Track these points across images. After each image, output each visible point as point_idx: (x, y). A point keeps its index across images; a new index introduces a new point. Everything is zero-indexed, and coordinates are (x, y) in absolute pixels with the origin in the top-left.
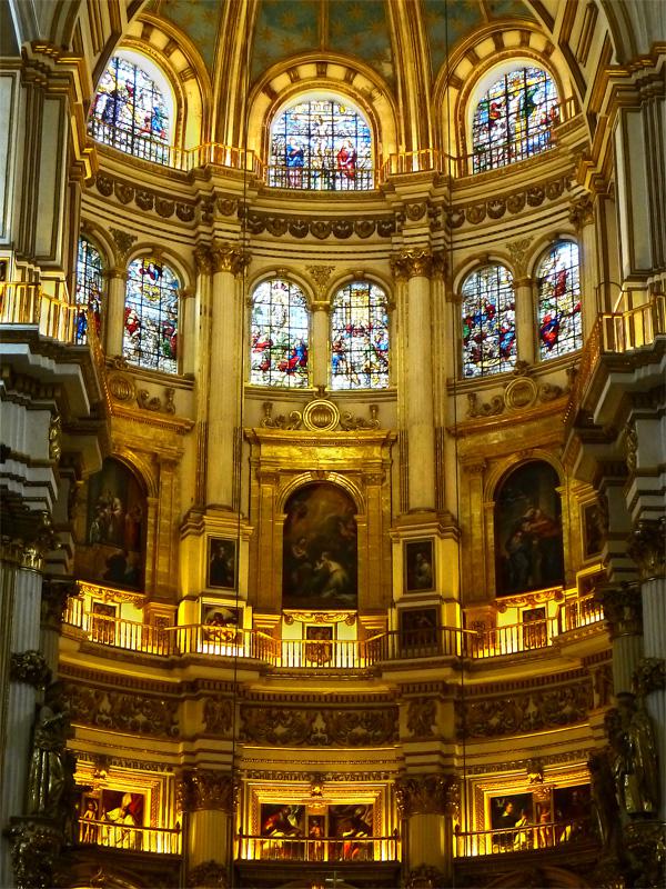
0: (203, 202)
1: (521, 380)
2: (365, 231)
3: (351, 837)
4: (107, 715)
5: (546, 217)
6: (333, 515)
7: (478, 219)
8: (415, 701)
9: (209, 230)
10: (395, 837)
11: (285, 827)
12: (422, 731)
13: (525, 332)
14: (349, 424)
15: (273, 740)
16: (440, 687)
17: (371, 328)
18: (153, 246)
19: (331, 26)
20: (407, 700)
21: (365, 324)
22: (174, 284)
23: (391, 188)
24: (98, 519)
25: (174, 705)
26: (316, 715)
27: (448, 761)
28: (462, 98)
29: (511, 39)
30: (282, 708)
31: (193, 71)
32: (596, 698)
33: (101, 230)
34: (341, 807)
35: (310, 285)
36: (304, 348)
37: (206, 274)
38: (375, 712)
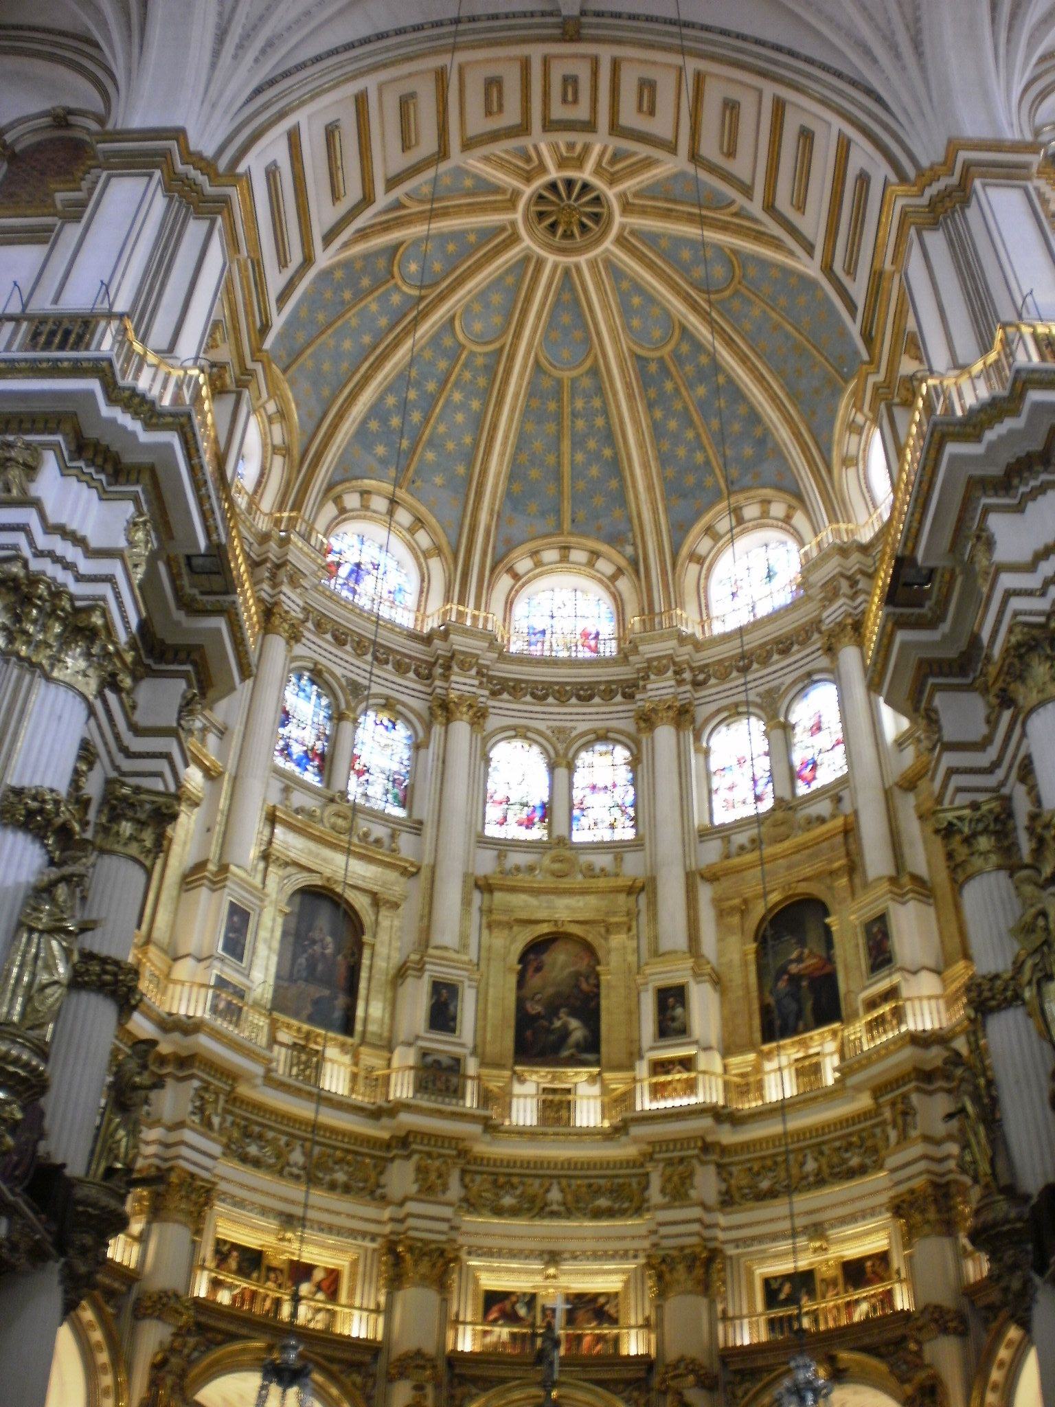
0: (441, 661)
1: (780, 815)
2: (608, 694)
4: (299, 1168)
5: (795, 662)
6: (572, 969)
7: (724, 677)
8: (670, 1162)
9: (445, 685)
10: (647, 1325)
12: (678, 1192)
13: (782, 771)
14: (590, 872)
15: (498, 1212)
16: (700, 1144)
17: (614, 786)
18: (387, 698)
19: (573, 512)
20: (658, 1161)
21: (609, 785)
22: (409, 737)
23: (635, 650)
24: (305, 955)
25: (382, 1165)
26: (551, 1185)
27: (707, 1233)
28: (704, 572)
29: (751, 511)
30: (510, 1175)
31: (438, 550)
32: (893, 1135)
33: (332, 674)
35: (551, 744)
36: (543, 806)
37: (441, 723)
38: (621, 1181)
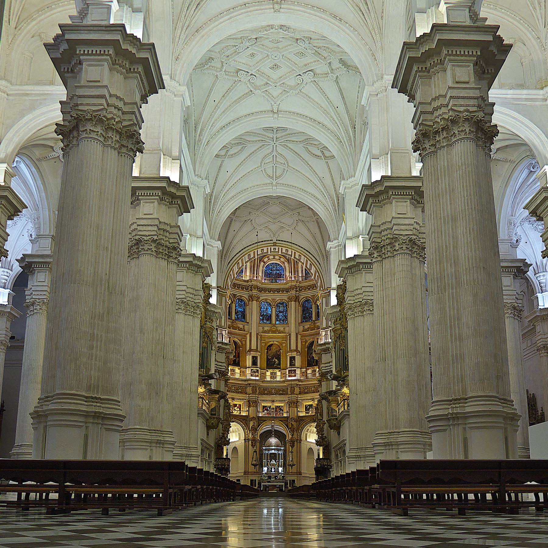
2: (283, 291)
3: (279, 412)
11: (267, 410)
12: (293, 393)
34: (277, 406)
